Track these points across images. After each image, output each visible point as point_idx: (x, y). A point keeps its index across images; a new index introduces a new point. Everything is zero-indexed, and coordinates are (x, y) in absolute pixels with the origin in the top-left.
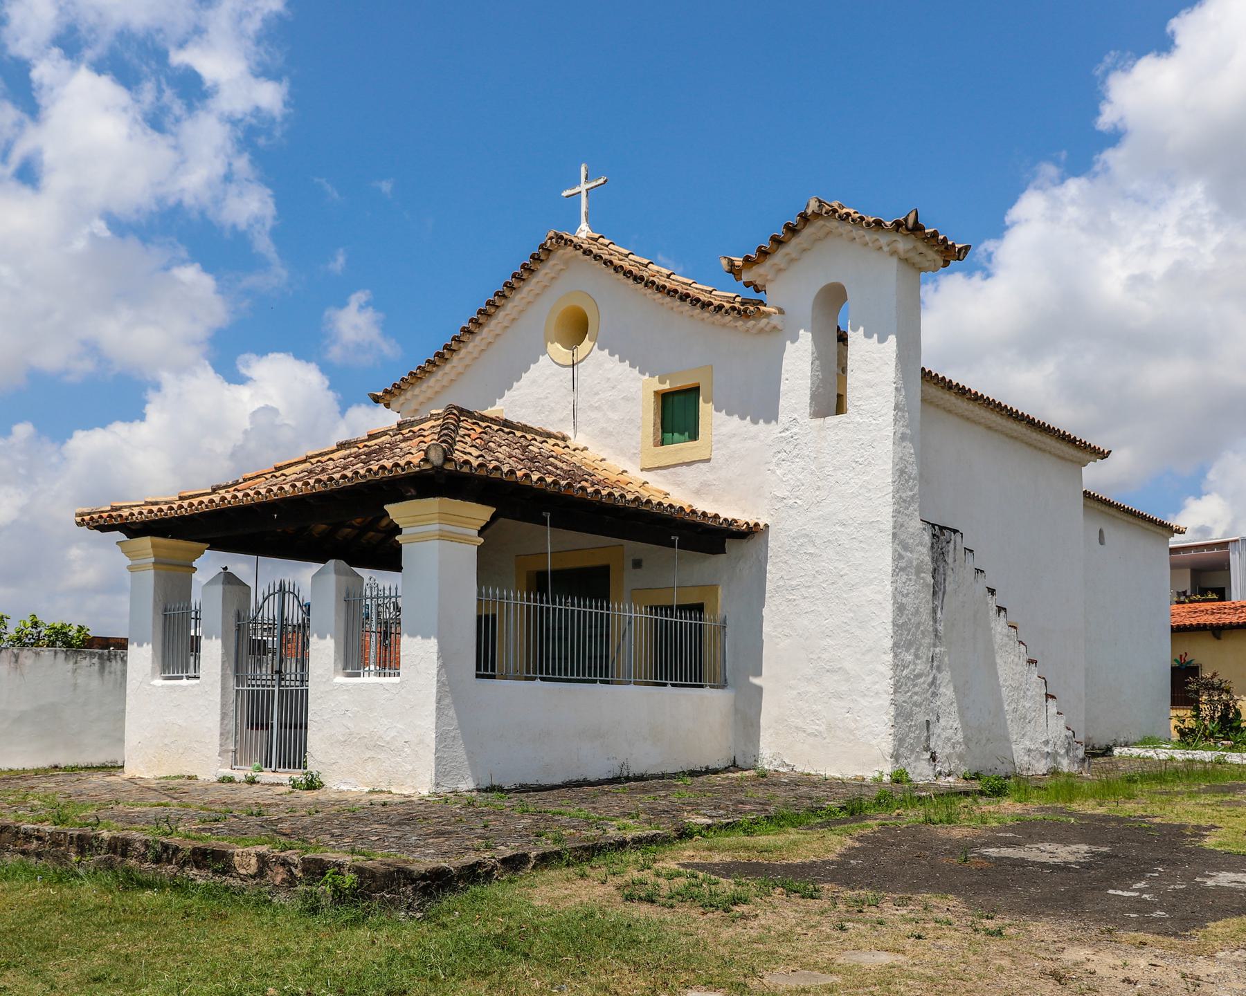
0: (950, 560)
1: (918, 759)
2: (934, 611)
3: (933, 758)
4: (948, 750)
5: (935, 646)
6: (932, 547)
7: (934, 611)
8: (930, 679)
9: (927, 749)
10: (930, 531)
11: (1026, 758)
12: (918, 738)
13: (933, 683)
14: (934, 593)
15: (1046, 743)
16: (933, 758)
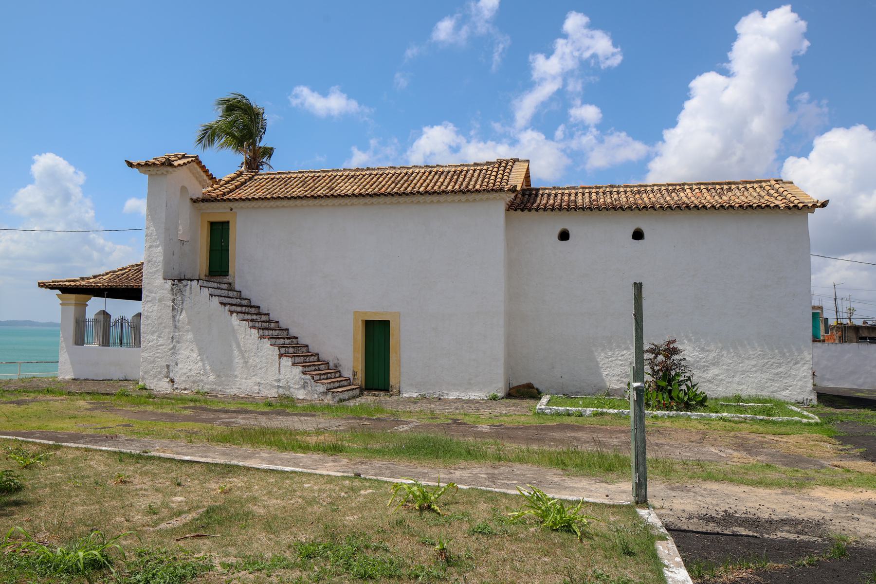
0: (187, 294)
1: (160, 380)
2: (174, 317)
3: (172, 381)
4: (183, 379)
5: (174, 332)
6: (172, 289)
7: (174, 317)
8: (171, 346)
9: (167, 377)
10: (170, 282)
11: (256, 387)
12: (160, 372)
13: (174, 348)
14: (173, 309)
15: (279, 380)
16: (172, 381)
